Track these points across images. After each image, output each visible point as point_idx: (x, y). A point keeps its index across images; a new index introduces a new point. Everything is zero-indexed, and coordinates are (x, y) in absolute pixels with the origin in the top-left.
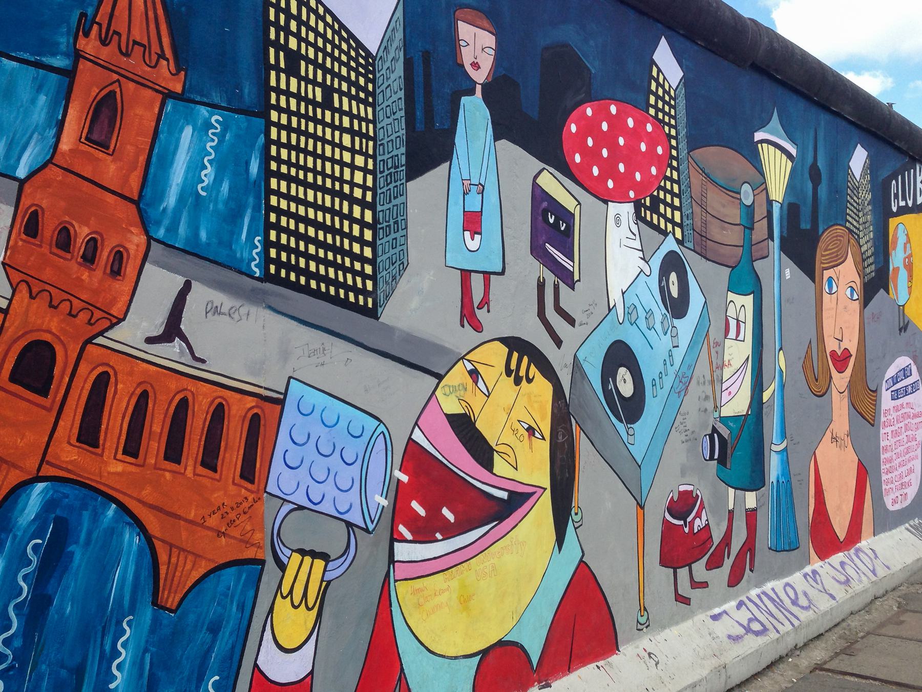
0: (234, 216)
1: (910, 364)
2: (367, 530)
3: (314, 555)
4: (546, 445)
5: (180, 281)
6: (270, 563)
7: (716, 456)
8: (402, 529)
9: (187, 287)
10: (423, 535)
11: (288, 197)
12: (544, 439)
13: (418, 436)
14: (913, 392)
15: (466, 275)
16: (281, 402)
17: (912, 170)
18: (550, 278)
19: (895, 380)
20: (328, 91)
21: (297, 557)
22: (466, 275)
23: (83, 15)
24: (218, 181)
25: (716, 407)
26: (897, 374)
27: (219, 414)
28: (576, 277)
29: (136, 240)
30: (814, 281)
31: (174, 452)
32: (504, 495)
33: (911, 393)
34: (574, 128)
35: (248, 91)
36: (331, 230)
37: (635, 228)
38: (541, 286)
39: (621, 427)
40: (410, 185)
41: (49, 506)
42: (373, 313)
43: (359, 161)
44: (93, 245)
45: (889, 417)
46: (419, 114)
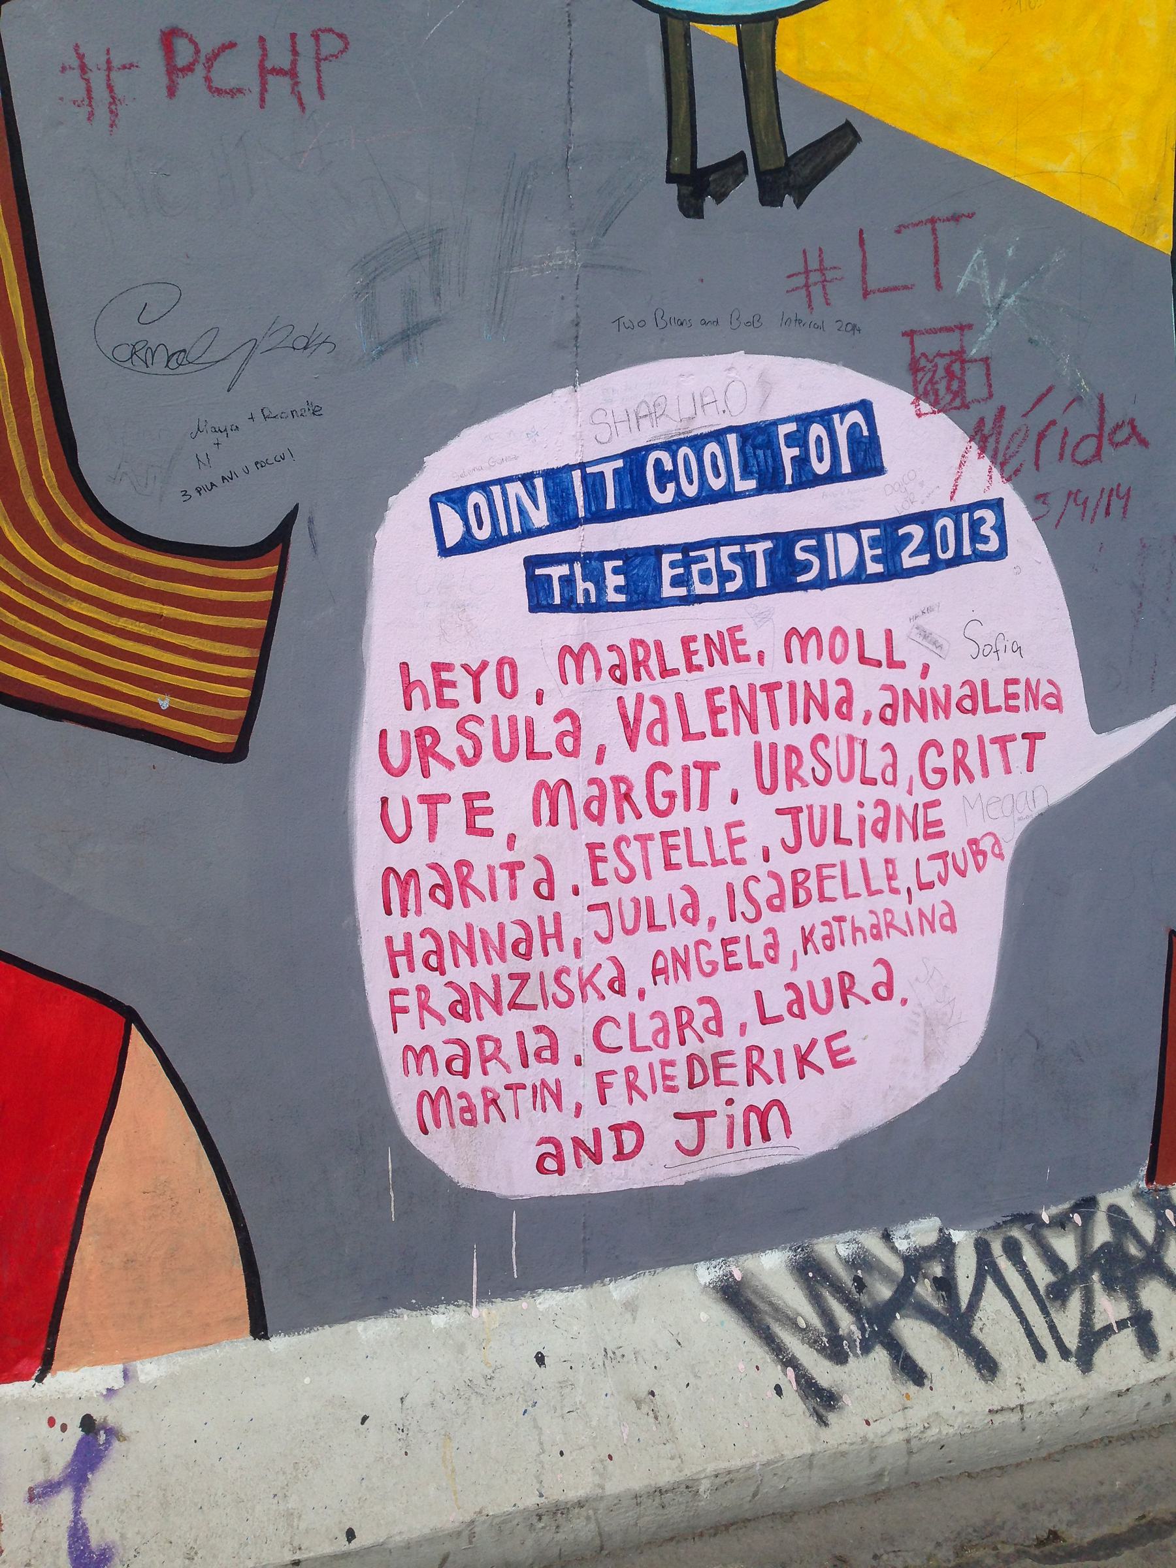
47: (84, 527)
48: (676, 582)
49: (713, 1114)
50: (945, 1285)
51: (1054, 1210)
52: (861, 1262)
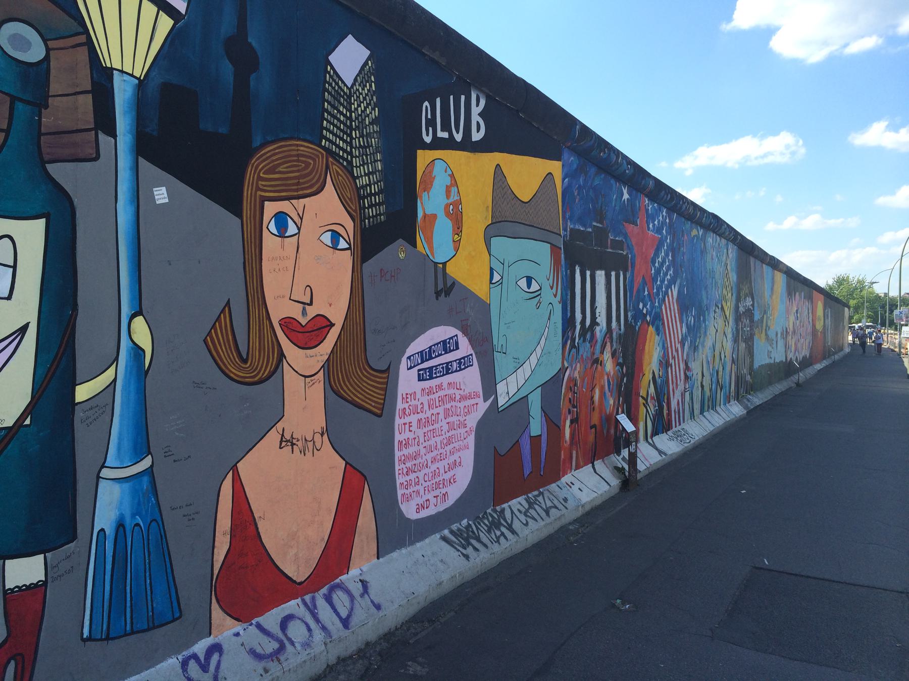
1: (456, 335)
14: (461, 370)
17: (463, 97)
19: (426, 355)
26: (430, 347)
30: (238, 213)
33: (456, 371)
45: (414, 403)
47: (366, 367)
48: (435, 373)
49: (438, 496)
50: (473, 532)
51: (482, 515)
52: (459, 530)
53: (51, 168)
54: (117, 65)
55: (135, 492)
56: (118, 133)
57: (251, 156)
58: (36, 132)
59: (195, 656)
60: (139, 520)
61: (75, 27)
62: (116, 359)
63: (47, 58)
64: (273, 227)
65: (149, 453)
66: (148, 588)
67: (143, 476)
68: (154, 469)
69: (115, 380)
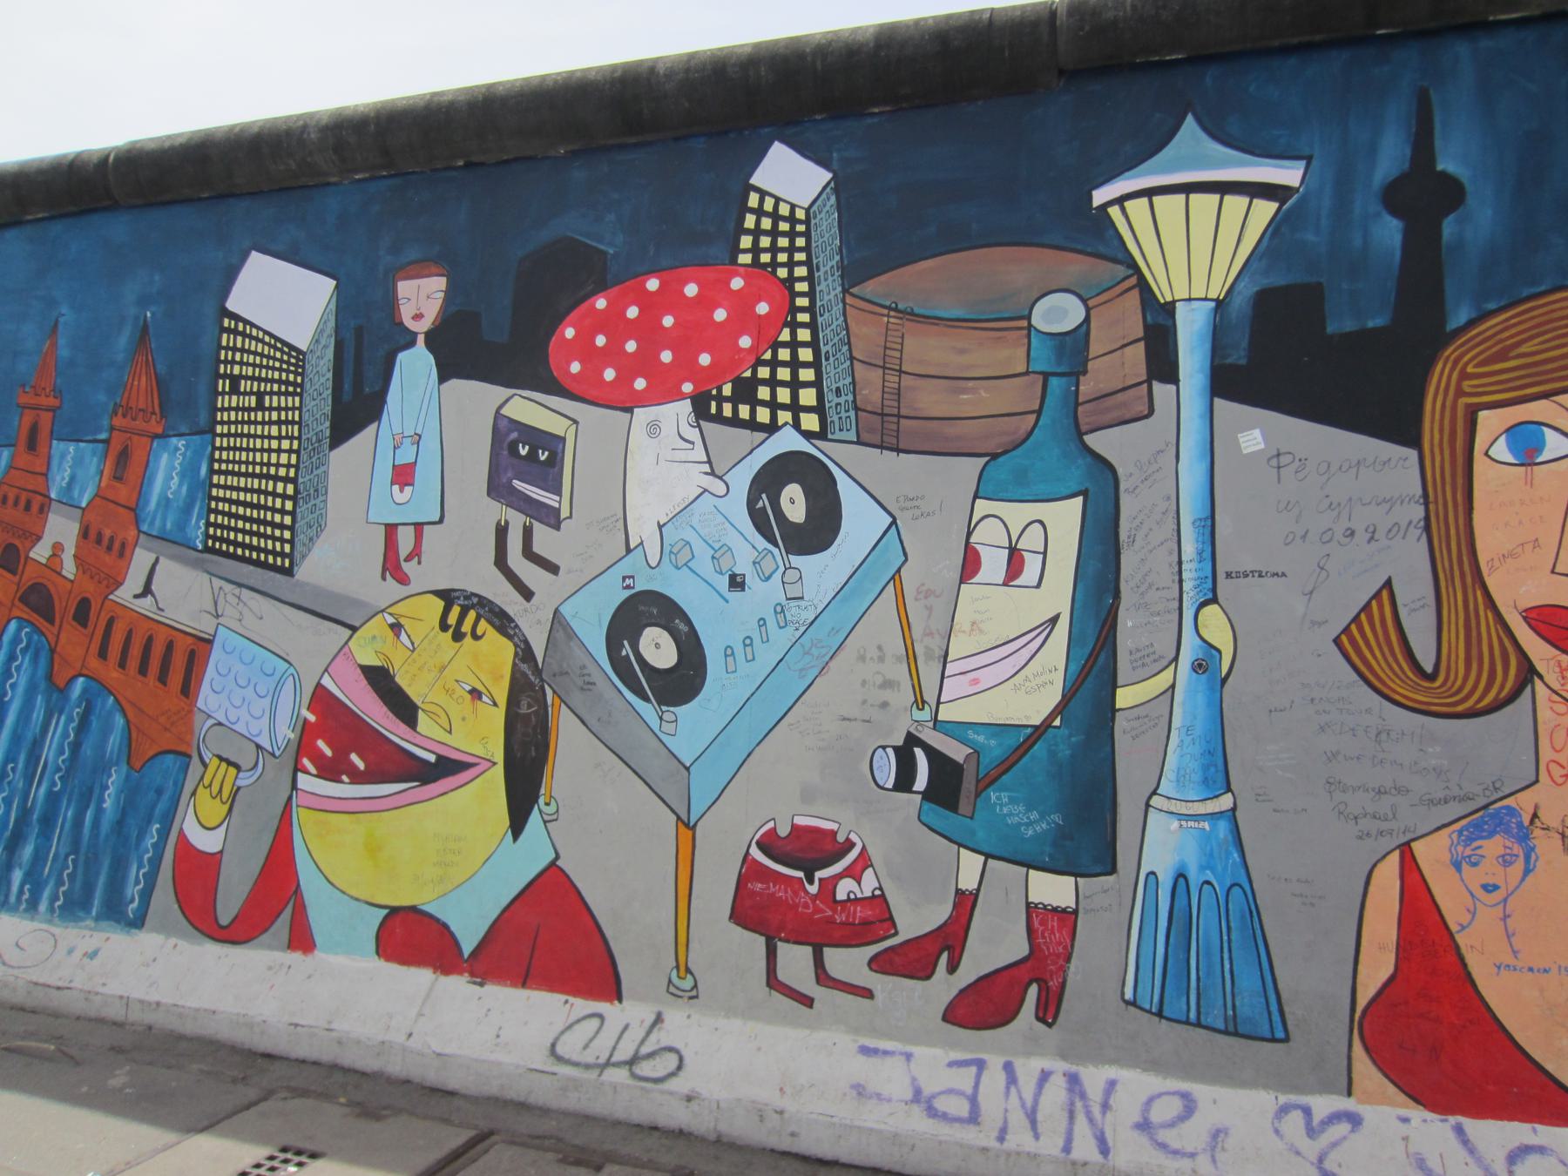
0: (187, 510)
2: (273, 755)
3: (230, 763)
4: (498, 717)
5: (154, 556)
6: (195, 759)
7: (921, 782)
8: (306, 762)
9: (157, 560)
10: (330, 771)
11: (225, 487)
12: (495, 704)
13: (327, 682)
15: (391, 530)
16: (210, 642)
18: (517, 520)
20: (260, 396)
21: (216, 761)
22: (391, 530)
23: (116, 404)
24: (180, 485)
25: (920, 703)
27: (170, 646)
28: (564, 513)
29: (134, 532)
31: (143, 670)
32: (432, 758)
34: (570, 333)
35: (203, 418)
36: (258, 507)
37: (693, 434)
38: (502, 532)
39: (648, 710)
40: (332, 453)
41: (85, 691)
42: (289, 572)
43: (285, 444)
44: (112, 539)
46: (347, 386)
53: (1090, 440)
54: (1180, 293)
55: (1206, 837)
56: (1181, 378)
57: (1446, 345)
58: (1074, 402)
59: (1307, 1111)
60: (1209, 876)
61: (1121, 271)
62: (1176, 659)
63: (1087, 320)
64: (1501, 450)
65: (1229, 789)
66: (1227, 975)
67: (1218, 819)
68: (1237, 813)
69: (1173, 686)
